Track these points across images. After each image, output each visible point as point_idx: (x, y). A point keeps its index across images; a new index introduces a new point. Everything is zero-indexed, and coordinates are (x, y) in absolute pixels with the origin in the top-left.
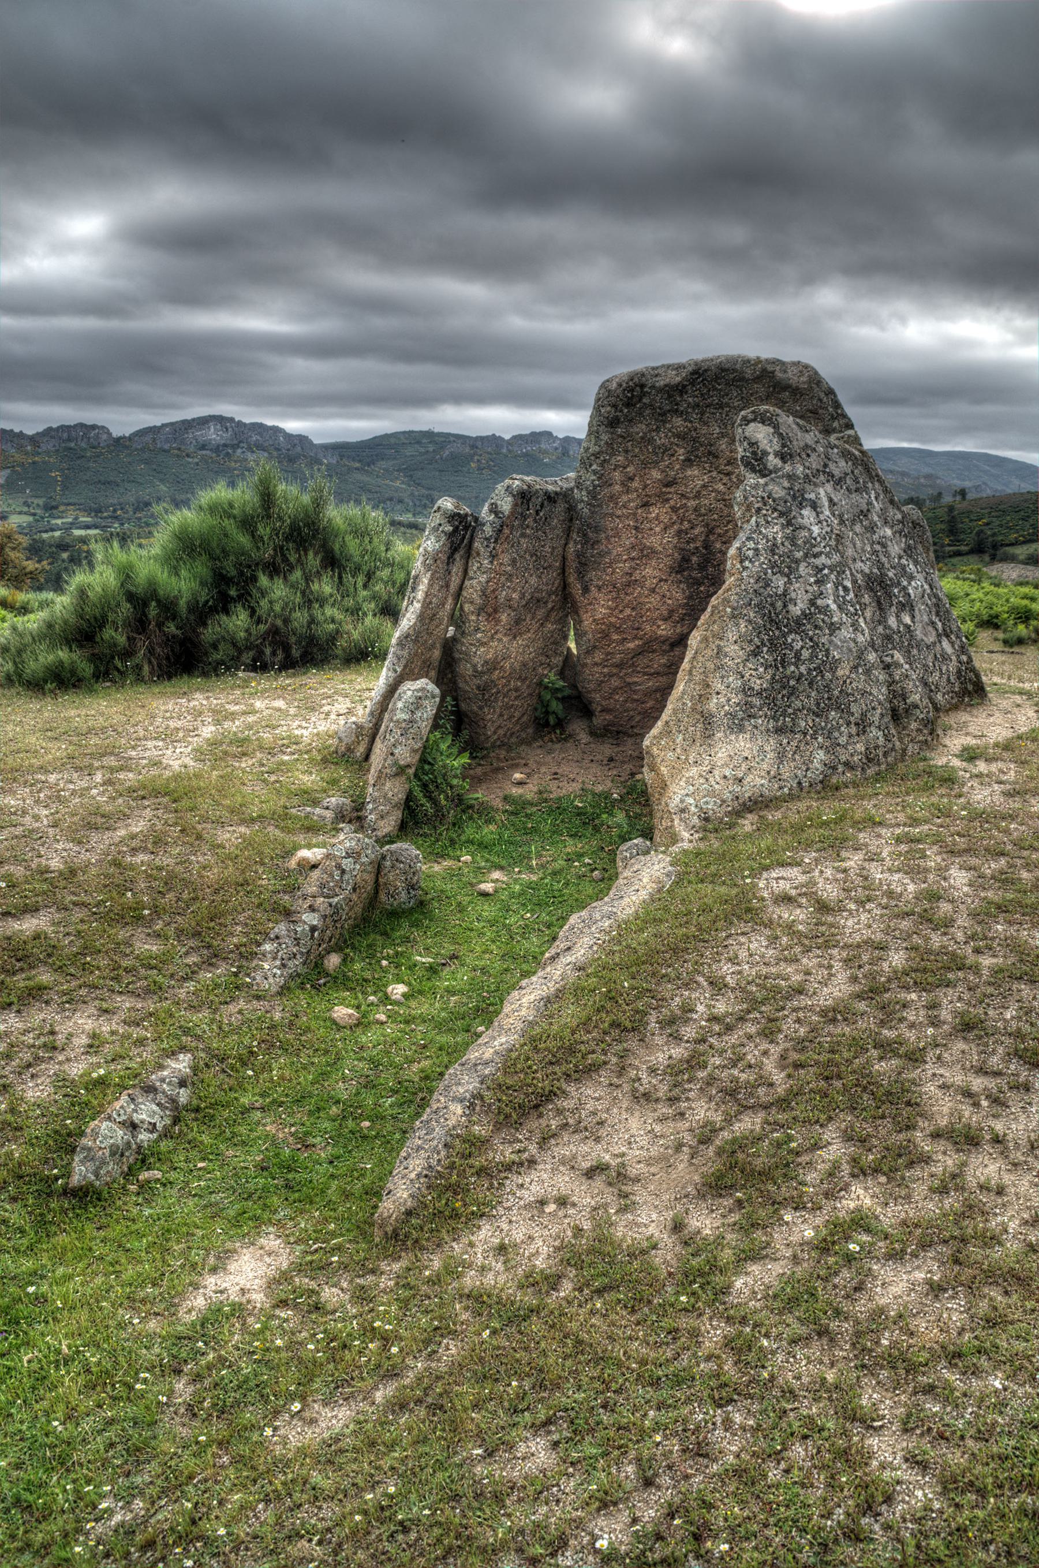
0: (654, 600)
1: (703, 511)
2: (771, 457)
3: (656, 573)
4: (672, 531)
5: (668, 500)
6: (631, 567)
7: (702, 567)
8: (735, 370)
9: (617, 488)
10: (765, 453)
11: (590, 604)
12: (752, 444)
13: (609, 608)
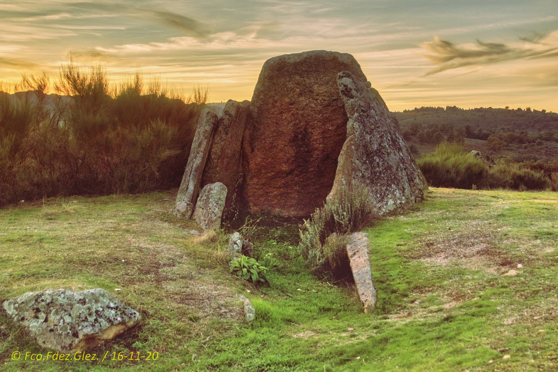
0: (281, 155)
1: (305, 115)
2: (353, 90)
3: (284, 143)
4: (291, 124)
5: (291, 111)
6: (273, 140)
7: (303, 139)
8: (322, 57)
9: (270, 105)
10: (351, 89)
11: (254, 157)
12: (345, 86)
13: (262, 158)
